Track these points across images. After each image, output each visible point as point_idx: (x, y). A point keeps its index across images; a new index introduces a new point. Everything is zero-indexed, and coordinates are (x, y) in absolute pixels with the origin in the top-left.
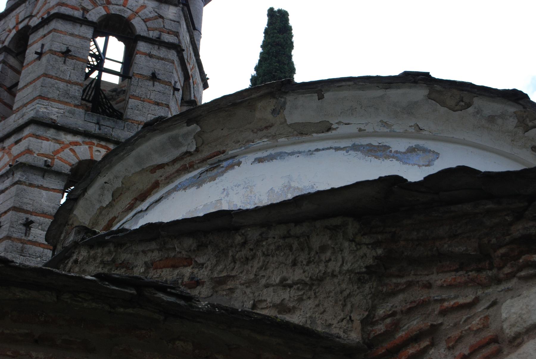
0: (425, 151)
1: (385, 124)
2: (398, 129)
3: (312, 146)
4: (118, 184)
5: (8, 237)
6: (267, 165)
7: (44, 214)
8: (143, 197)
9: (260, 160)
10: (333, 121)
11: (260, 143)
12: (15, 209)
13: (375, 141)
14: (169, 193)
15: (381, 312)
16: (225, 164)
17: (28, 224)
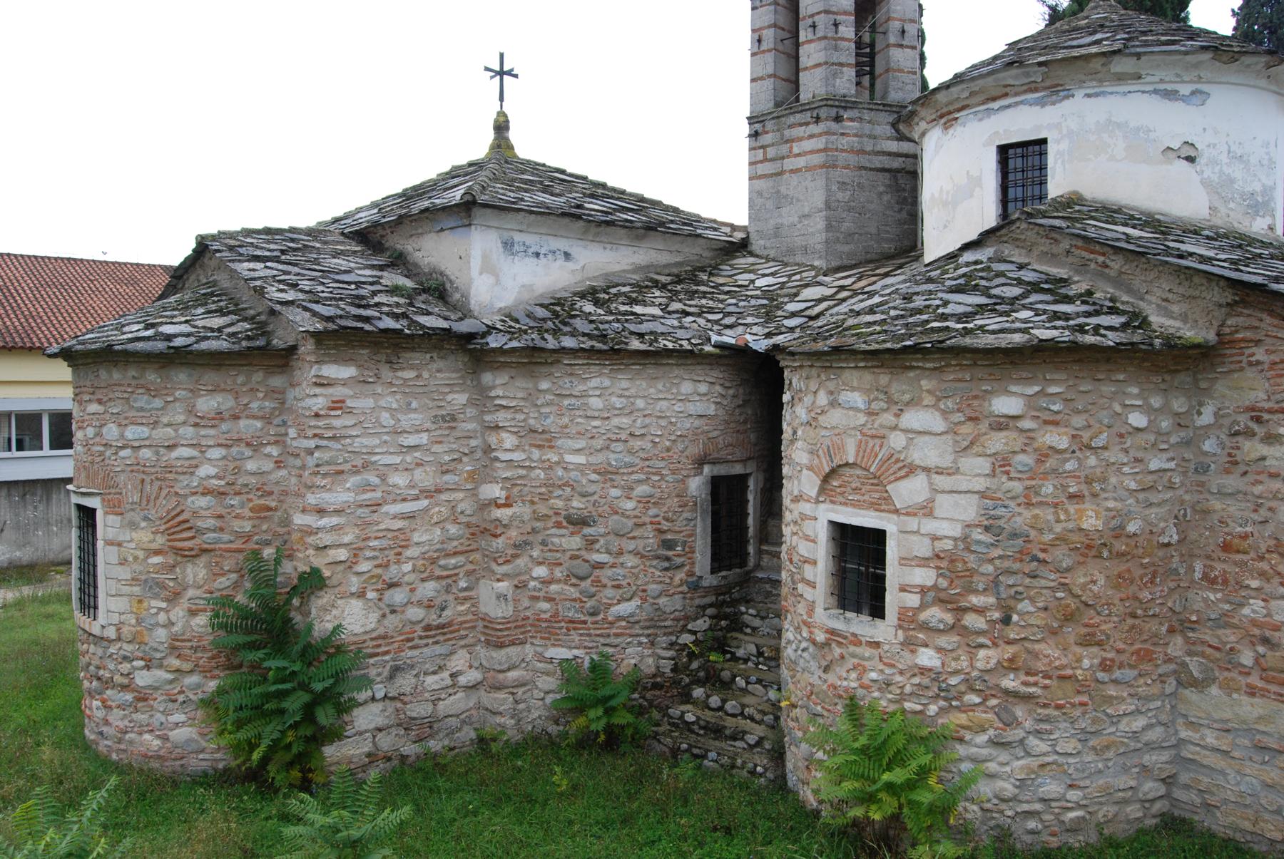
0: (1201, 92)
1: (1178, 75)
2: (1186, 78)
3: (1127, 88)
4: (977, 89)
5: (825, 38)
6: (1093, 100)
7: (845, 13)
8: (994, 99)
9: (1088, 96)
10: (1143, 73)
11: (1090, 84)
12: (827, 12)
13: (1169, 87)
14: (1017, 104)
15: (1229, 322)
16: (1062, 94)
17: (836, 25)
